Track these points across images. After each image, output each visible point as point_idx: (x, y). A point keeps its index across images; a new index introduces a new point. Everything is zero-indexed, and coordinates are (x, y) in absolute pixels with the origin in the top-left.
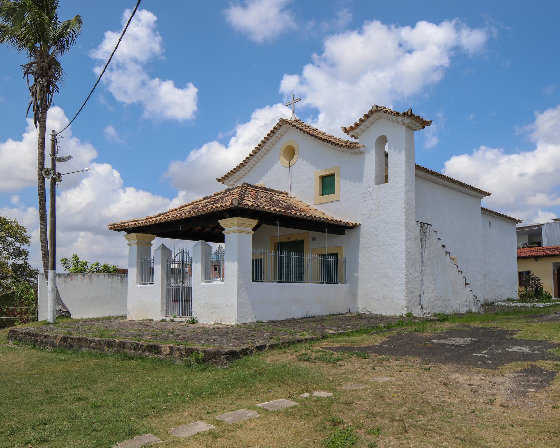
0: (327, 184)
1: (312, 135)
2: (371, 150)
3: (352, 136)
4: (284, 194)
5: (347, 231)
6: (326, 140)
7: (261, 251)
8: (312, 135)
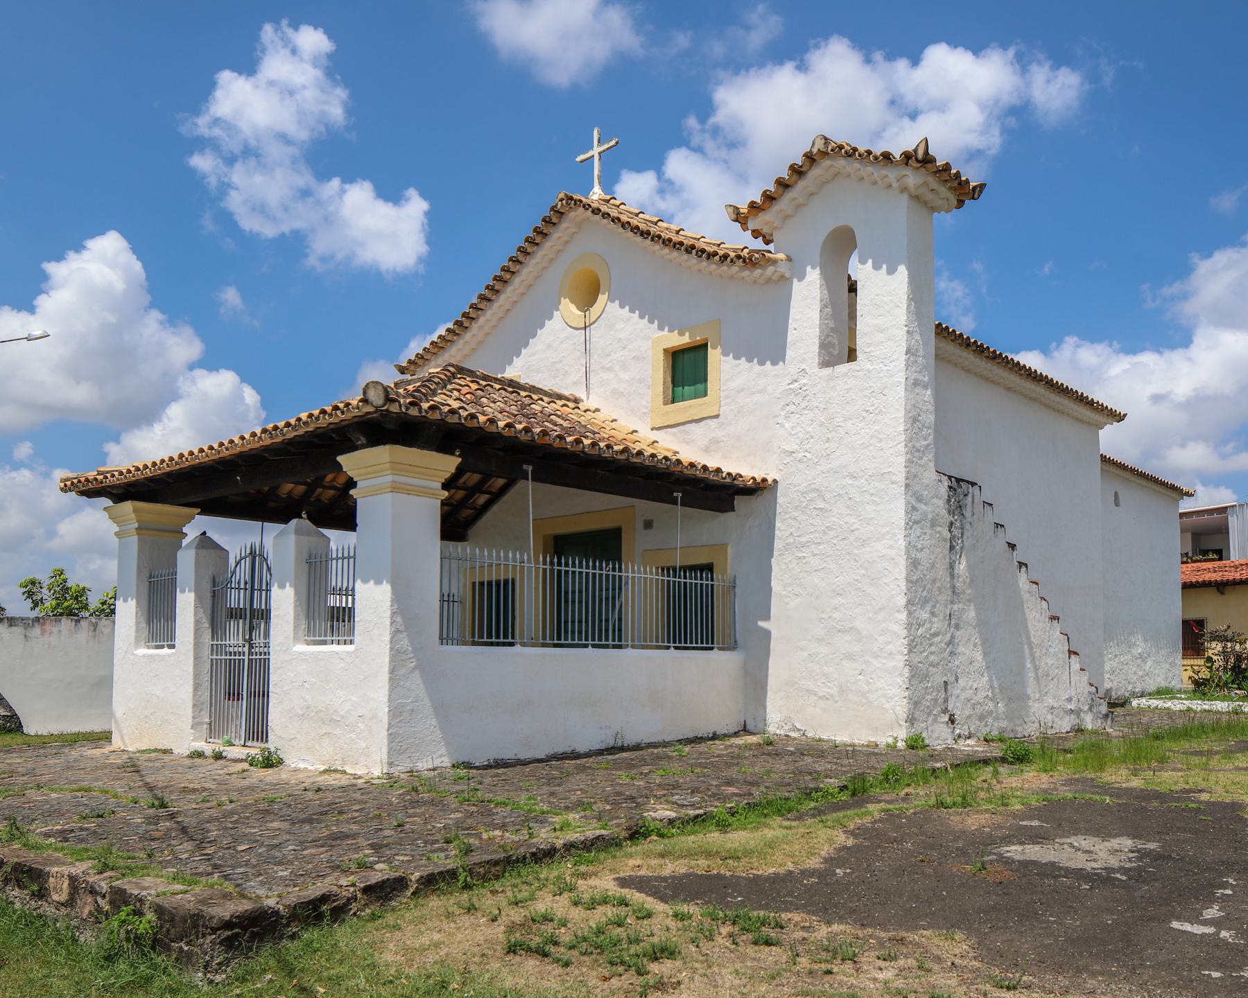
0: (686, 370)
1: (645, 234)
2: (809, 269)
3: (756, 234)
4: (568, 400)
5: (739, 501)
6: (681, 244)
7: (514, 556)
8: (645, 234)
